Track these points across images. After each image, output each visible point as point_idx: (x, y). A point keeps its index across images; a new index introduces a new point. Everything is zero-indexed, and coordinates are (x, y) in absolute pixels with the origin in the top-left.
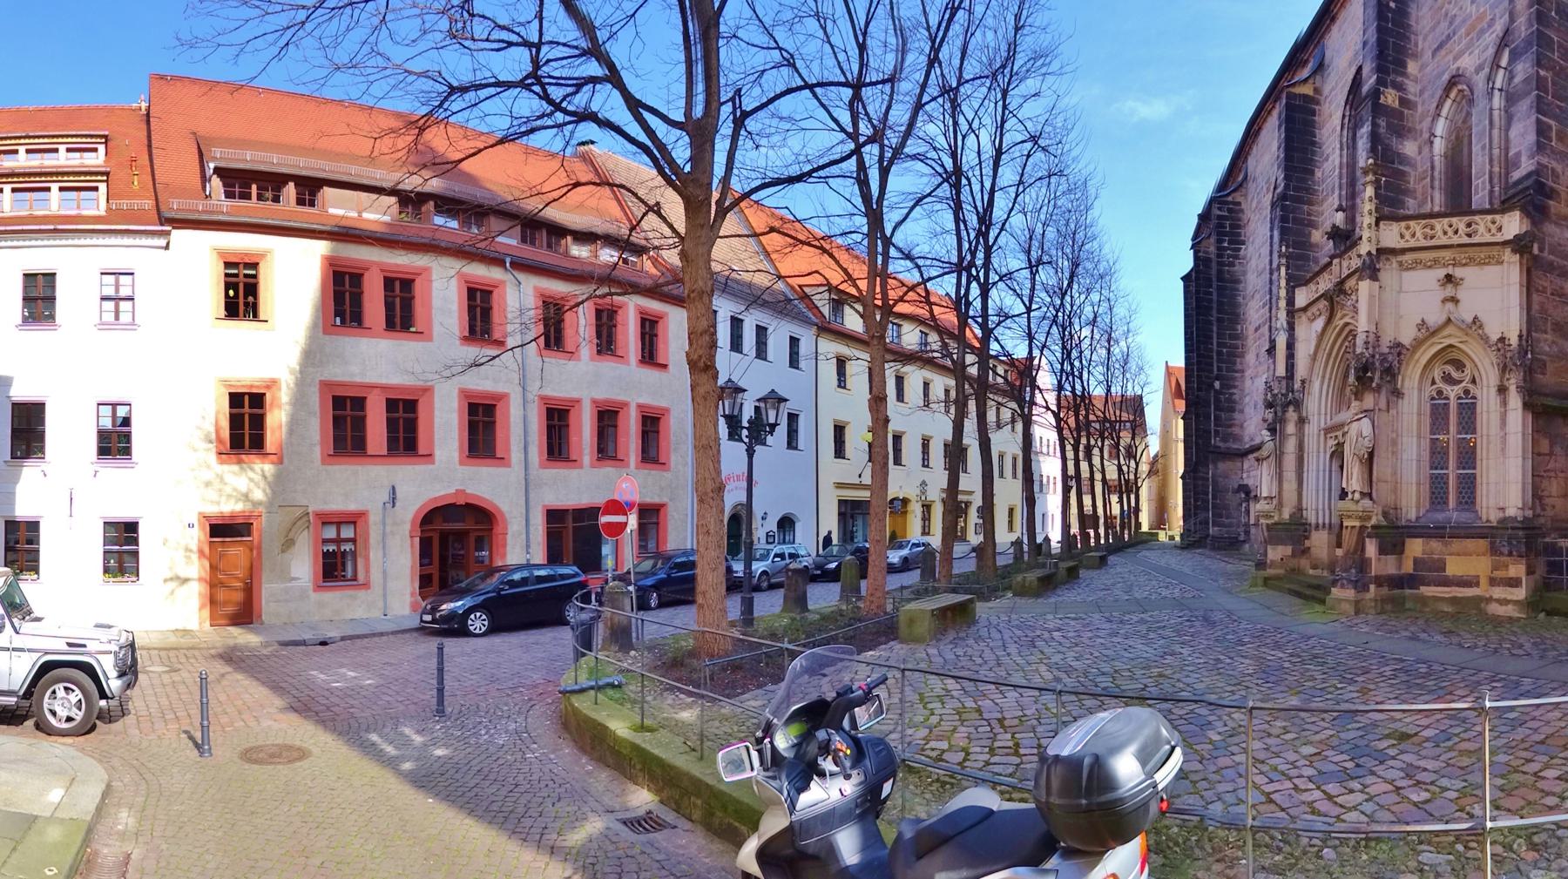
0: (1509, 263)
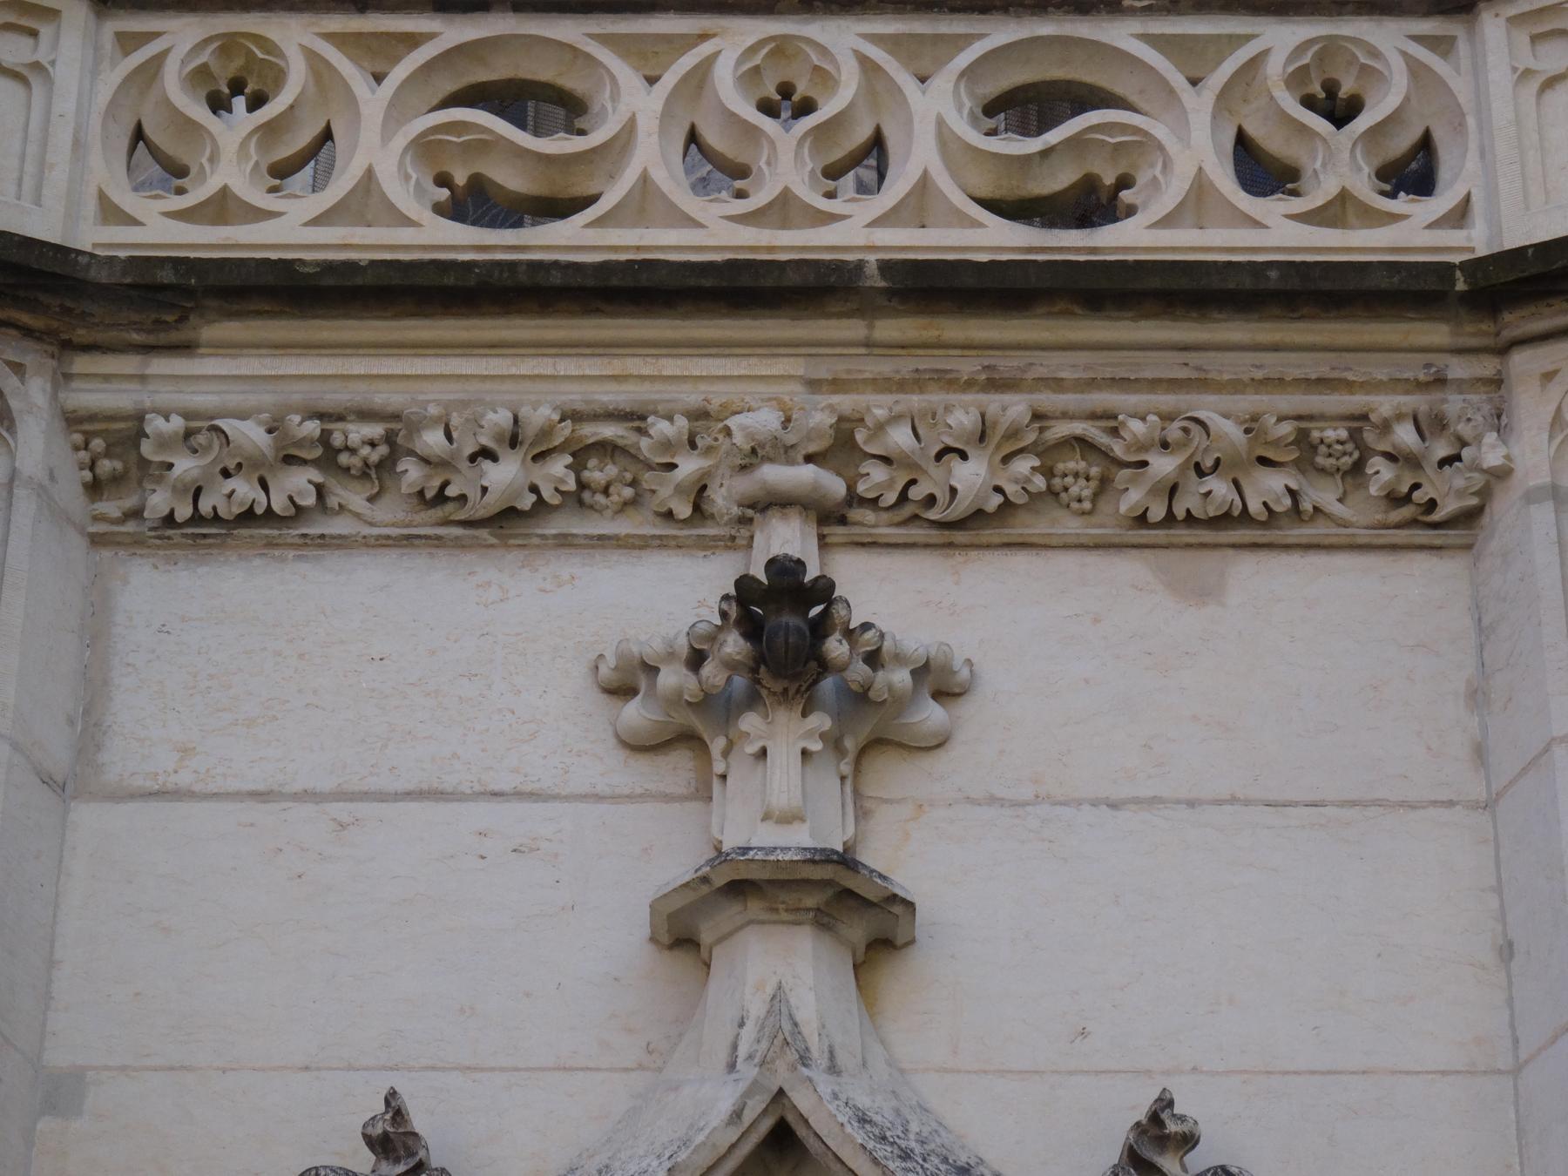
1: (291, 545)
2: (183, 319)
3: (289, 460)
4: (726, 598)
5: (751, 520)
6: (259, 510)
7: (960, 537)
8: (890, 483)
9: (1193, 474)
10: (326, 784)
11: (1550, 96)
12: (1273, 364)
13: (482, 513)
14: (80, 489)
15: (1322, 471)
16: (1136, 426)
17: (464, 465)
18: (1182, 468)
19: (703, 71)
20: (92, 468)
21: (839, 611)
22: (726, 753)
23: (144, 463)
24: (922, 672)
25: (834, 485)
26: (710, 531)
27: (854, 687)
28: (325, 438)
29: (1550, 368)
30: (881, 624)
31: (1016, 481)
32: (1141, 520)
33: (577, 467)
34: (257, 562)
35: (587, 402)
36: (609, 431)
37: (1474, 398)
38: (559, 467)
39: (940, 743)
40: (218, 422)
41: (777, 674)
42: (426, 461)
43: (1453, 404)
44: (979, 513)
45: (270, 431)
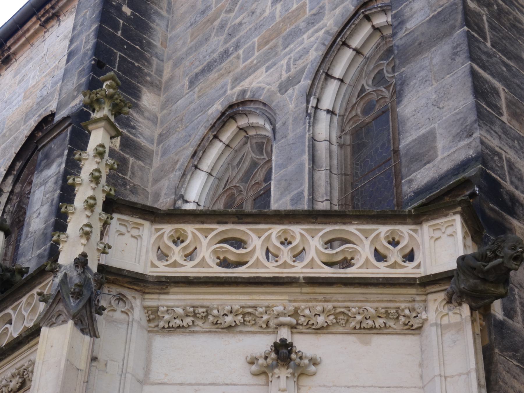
0: (443, 328)
1: (188, 333)
2: (167, 287)
3: (187, 316)
4: (272, 346)
5: (277, 328)
6: (181, 326)
7: (319, 331)
8: (305, 321)
9: (365, 319)
10: (193, 382)
11: (437, 242)
12: (381, 297)
13: (224, 327)
14: (146, 321)
15: (391, 318)
16: (353, 310)
17: (221, 317)
18: (363, 318)
19: (269, 237)
20: (149, 317)
21: (294, 349)
22: (272, 377)
23: (159, 316)
24: (311, 360)
25: (294, 321)
26: (270, 330)
27: (297, 364)
28: (194, 311)
29: (436, 299)
30: (302, 351)
31: (330, 321)
32: (355, 328)
33: (243, 317)
34: (181, 336)
35: (246, 304)
36: (250, 310)
37: (420, 304)
38: (240, 317)
39: (314, 374)
40: (173, 308)
41: (282, 361)
42: (214, 316)
43: (416, 305)
44: (323, 327)
45: (183, 310)
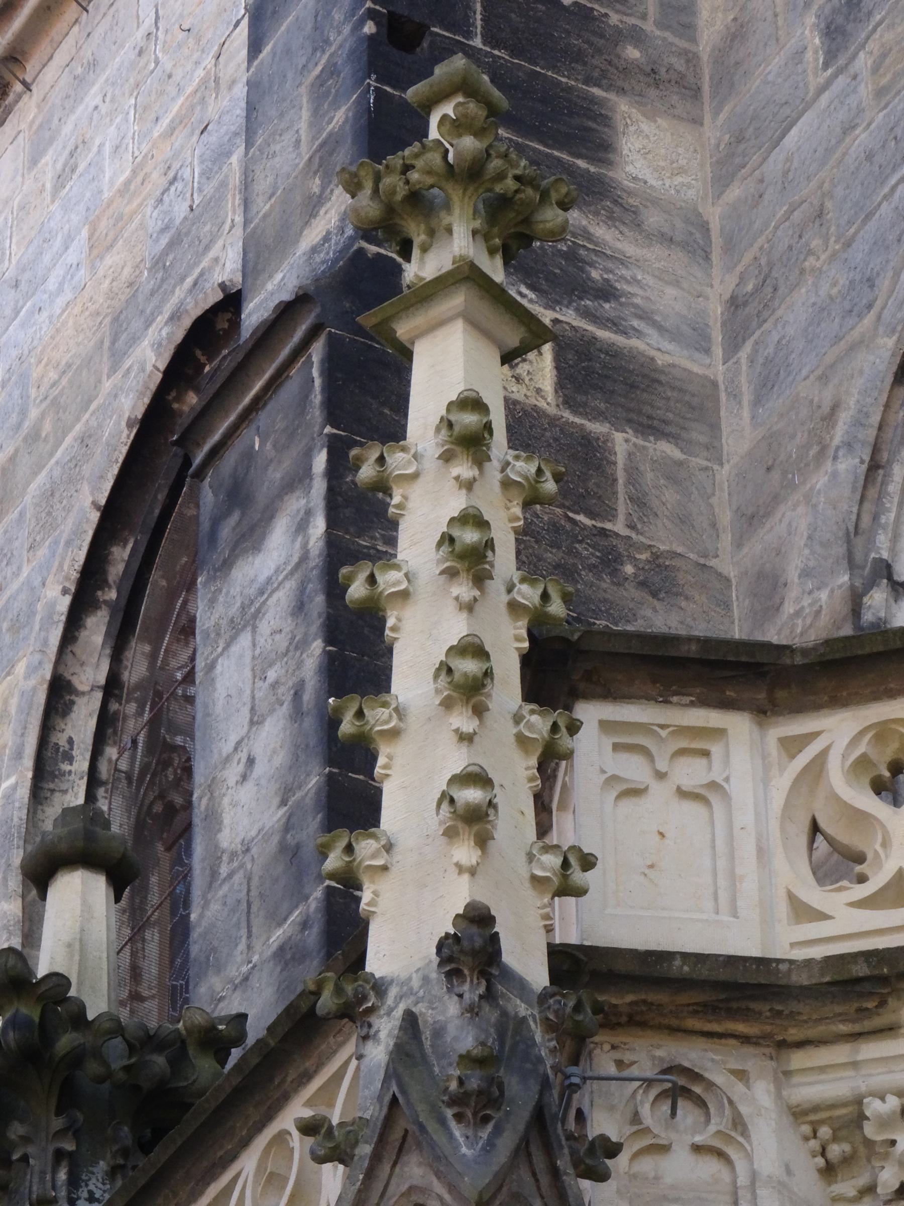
2: (883, 1003)
14: (816, 1175)
20: (823, 1154)
23: (869, 1144)
